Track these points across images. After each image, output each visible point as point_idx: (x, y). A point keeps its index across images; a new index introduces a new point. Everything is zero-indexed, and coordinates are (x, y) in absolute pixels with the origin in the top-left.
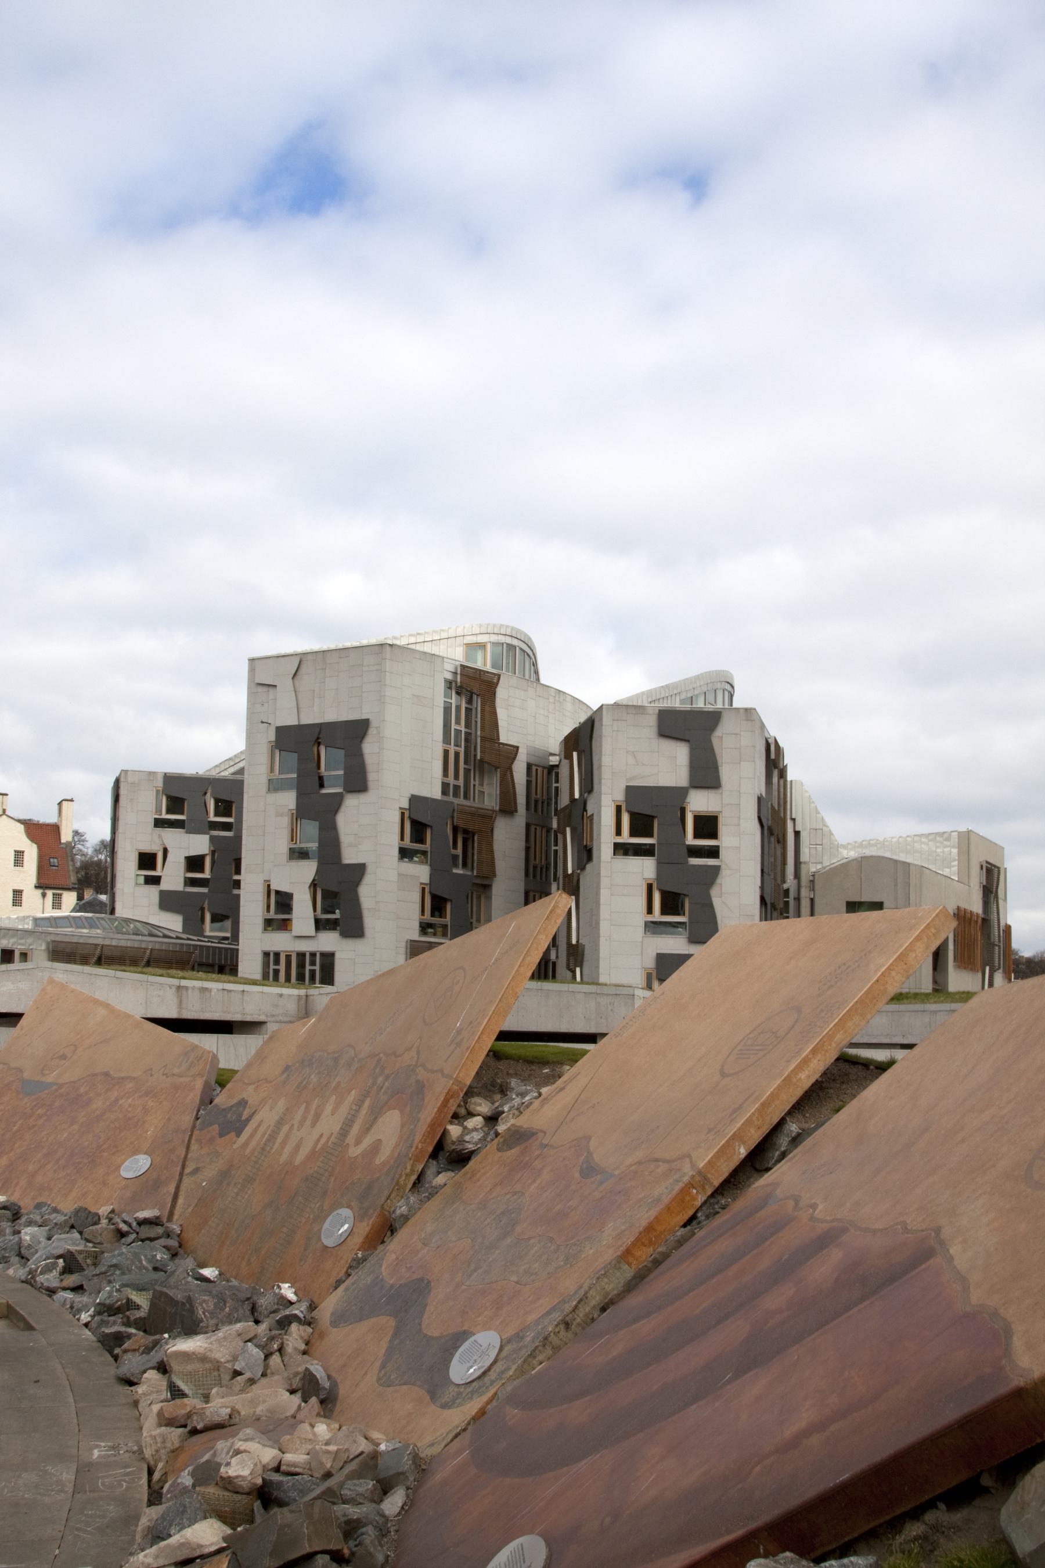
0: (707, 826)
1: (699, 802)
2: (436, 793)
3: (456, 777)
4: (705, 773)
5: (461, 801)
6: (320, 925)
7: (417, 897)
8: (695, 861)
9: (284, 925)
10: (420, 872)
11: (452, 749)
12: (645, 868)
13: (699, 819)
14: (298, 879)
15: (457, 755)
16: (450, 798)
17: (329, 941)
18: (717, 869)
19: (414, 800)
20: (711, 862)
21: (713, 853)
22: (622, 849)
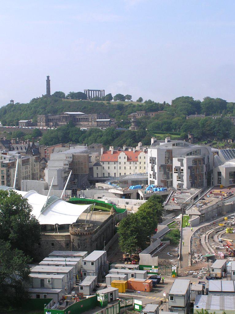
0: (182, 170)
1: (182, 168)
2: (164, 164)
3: (167, 161)
4: (182, 165)
5: (167, 164)
6: (153, 178)
7: (162, 175)
8: (181, 174)
9: (151, 178)
10: (163, 172)
11: (166, 159)
12: (177, 174)
13: (182, 169)
14: (152, 173)
15: (167, 159)
16: (167, 164)
17: (154, 180)
18: (183, 175)
19: (161, 165)
20: (182, 174)
21: (183, 173)
22: (175, 172)
